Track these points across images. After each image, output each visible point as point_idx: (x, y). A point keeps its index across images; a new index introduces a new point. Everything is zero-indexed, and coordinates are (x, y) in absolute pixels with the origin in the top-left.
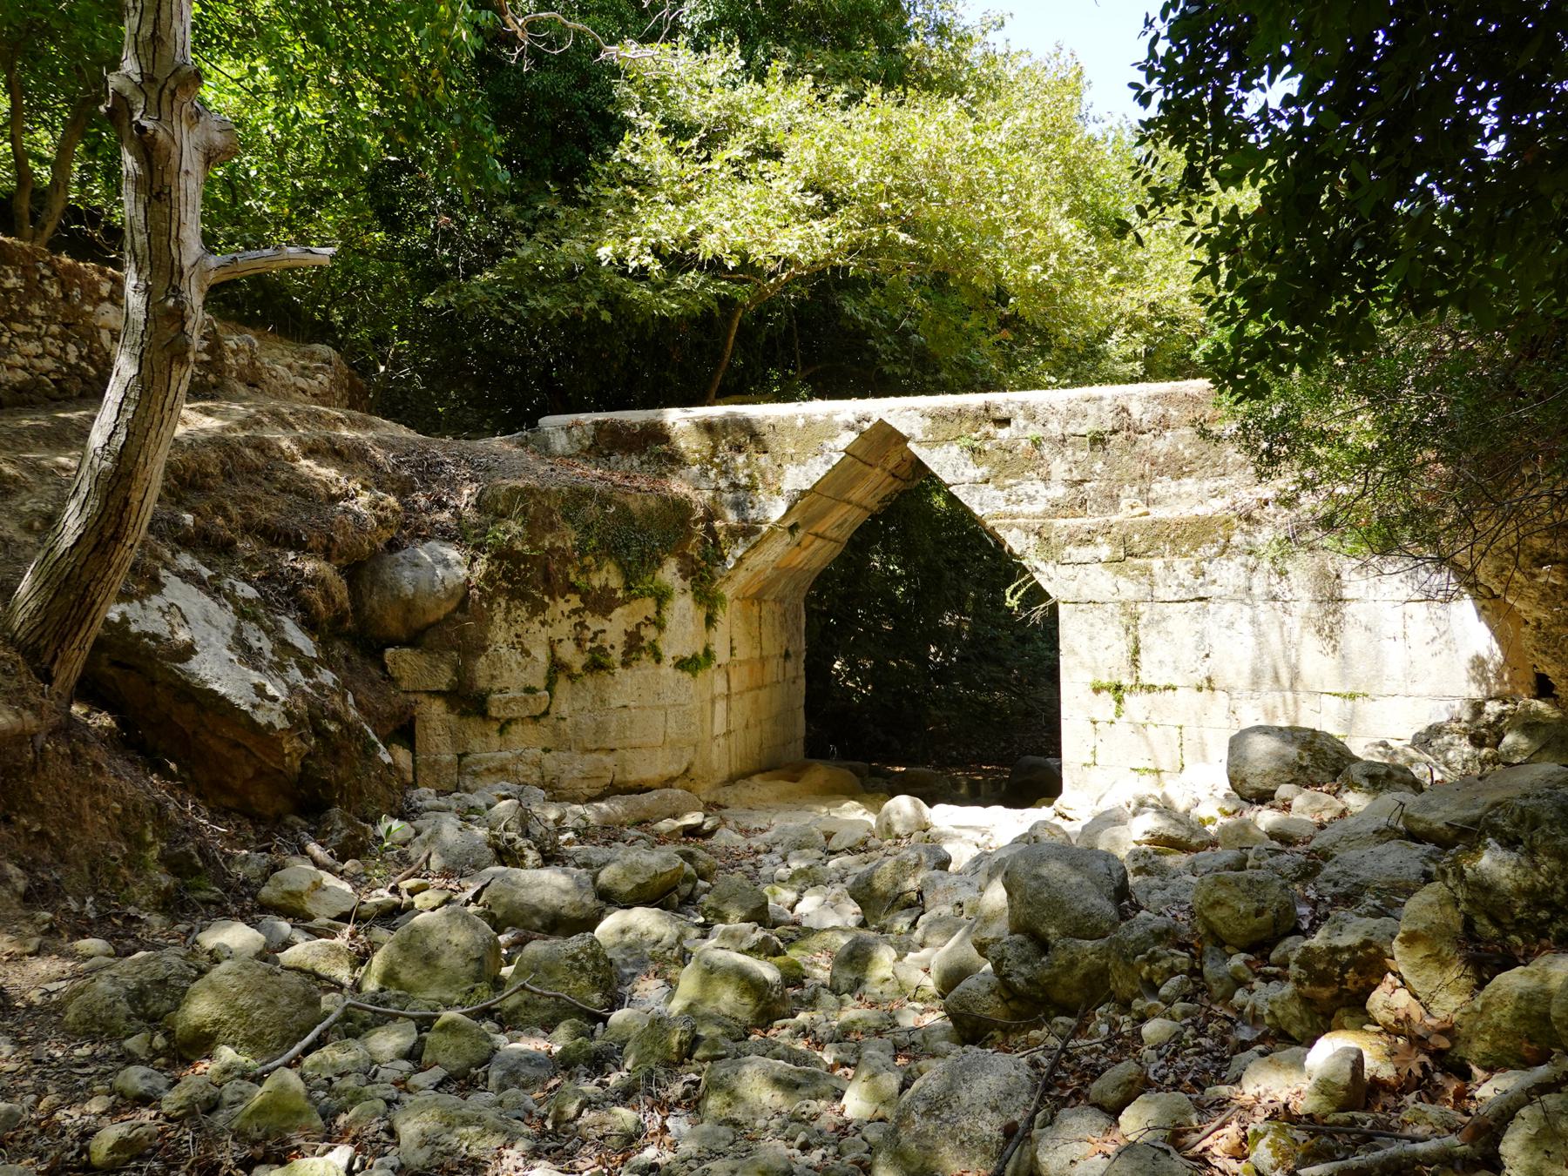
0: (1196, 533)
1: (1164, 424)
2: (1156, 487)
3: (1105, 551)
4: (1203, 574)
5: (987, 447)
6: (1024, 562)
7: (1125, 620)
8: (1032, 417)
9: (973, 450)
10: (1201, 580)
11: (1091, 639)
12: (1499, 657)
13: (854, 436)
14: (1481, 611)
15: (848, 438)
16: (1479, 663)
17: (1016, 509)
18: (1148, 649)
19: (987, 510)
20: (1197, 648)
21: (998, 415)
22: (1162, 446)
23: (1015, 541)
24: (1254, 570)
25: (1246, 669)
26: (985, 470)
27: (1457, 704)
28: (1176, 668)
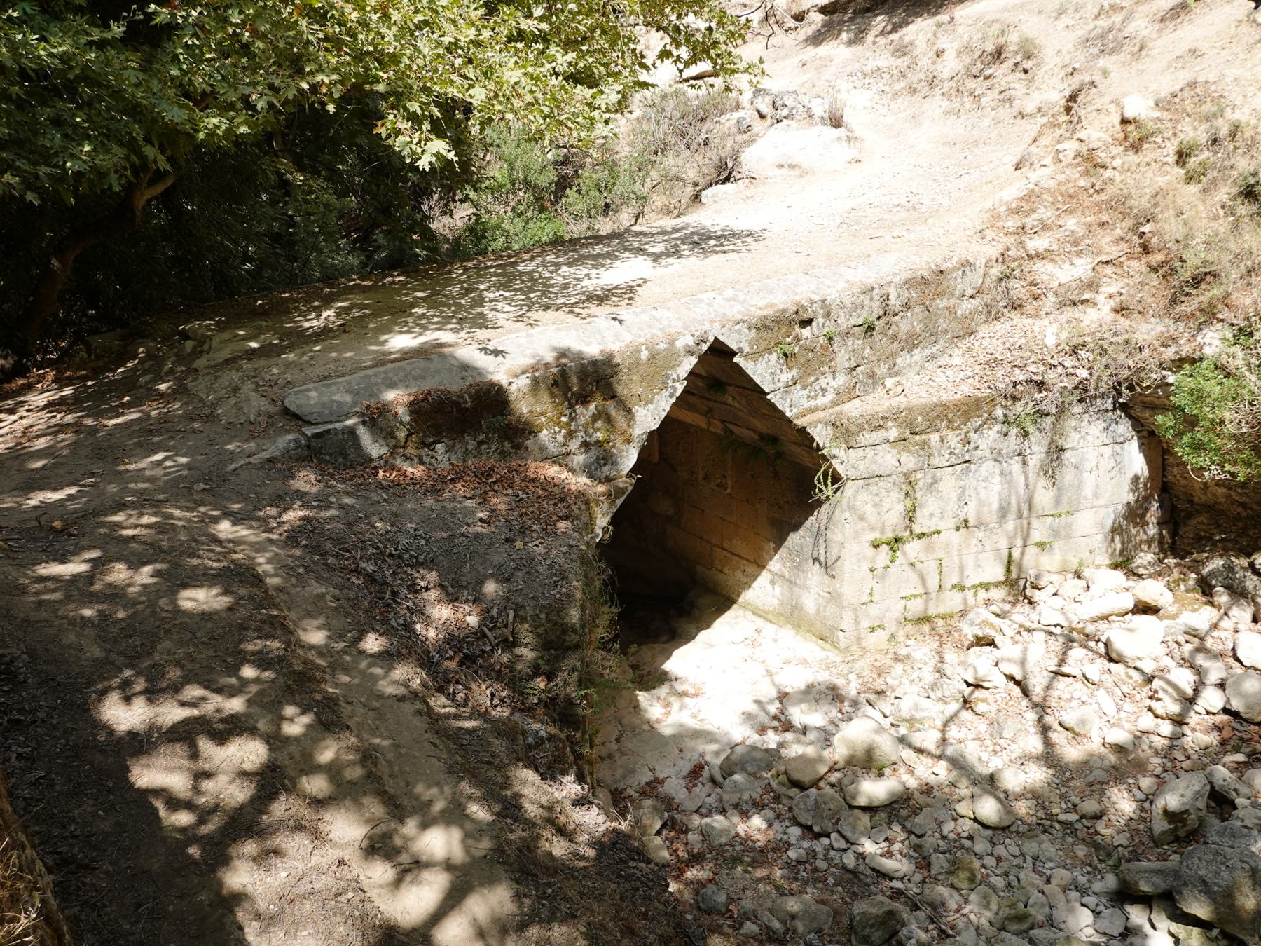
0: (969, 411)
1: (907, 306)
2: (899, 361)
3: (893, 433)
6: (825, 452)
7: (905, 487)
8: (828, 315)
9: (785, 355)
11: (875, 505)
12: (1146, 474)
14: (1141, 445)
15: (689, 363)
16: (1136, 479)
17: (813, 403)
18: (921, 506)
19: (795, 410)
21: (805, 317)
22: (903, 326)
23: (821, 435)
24: (1006, 435)
25: (995, 506)
26: (794, 372)
27: (1120, 507)
28: (942, 517)
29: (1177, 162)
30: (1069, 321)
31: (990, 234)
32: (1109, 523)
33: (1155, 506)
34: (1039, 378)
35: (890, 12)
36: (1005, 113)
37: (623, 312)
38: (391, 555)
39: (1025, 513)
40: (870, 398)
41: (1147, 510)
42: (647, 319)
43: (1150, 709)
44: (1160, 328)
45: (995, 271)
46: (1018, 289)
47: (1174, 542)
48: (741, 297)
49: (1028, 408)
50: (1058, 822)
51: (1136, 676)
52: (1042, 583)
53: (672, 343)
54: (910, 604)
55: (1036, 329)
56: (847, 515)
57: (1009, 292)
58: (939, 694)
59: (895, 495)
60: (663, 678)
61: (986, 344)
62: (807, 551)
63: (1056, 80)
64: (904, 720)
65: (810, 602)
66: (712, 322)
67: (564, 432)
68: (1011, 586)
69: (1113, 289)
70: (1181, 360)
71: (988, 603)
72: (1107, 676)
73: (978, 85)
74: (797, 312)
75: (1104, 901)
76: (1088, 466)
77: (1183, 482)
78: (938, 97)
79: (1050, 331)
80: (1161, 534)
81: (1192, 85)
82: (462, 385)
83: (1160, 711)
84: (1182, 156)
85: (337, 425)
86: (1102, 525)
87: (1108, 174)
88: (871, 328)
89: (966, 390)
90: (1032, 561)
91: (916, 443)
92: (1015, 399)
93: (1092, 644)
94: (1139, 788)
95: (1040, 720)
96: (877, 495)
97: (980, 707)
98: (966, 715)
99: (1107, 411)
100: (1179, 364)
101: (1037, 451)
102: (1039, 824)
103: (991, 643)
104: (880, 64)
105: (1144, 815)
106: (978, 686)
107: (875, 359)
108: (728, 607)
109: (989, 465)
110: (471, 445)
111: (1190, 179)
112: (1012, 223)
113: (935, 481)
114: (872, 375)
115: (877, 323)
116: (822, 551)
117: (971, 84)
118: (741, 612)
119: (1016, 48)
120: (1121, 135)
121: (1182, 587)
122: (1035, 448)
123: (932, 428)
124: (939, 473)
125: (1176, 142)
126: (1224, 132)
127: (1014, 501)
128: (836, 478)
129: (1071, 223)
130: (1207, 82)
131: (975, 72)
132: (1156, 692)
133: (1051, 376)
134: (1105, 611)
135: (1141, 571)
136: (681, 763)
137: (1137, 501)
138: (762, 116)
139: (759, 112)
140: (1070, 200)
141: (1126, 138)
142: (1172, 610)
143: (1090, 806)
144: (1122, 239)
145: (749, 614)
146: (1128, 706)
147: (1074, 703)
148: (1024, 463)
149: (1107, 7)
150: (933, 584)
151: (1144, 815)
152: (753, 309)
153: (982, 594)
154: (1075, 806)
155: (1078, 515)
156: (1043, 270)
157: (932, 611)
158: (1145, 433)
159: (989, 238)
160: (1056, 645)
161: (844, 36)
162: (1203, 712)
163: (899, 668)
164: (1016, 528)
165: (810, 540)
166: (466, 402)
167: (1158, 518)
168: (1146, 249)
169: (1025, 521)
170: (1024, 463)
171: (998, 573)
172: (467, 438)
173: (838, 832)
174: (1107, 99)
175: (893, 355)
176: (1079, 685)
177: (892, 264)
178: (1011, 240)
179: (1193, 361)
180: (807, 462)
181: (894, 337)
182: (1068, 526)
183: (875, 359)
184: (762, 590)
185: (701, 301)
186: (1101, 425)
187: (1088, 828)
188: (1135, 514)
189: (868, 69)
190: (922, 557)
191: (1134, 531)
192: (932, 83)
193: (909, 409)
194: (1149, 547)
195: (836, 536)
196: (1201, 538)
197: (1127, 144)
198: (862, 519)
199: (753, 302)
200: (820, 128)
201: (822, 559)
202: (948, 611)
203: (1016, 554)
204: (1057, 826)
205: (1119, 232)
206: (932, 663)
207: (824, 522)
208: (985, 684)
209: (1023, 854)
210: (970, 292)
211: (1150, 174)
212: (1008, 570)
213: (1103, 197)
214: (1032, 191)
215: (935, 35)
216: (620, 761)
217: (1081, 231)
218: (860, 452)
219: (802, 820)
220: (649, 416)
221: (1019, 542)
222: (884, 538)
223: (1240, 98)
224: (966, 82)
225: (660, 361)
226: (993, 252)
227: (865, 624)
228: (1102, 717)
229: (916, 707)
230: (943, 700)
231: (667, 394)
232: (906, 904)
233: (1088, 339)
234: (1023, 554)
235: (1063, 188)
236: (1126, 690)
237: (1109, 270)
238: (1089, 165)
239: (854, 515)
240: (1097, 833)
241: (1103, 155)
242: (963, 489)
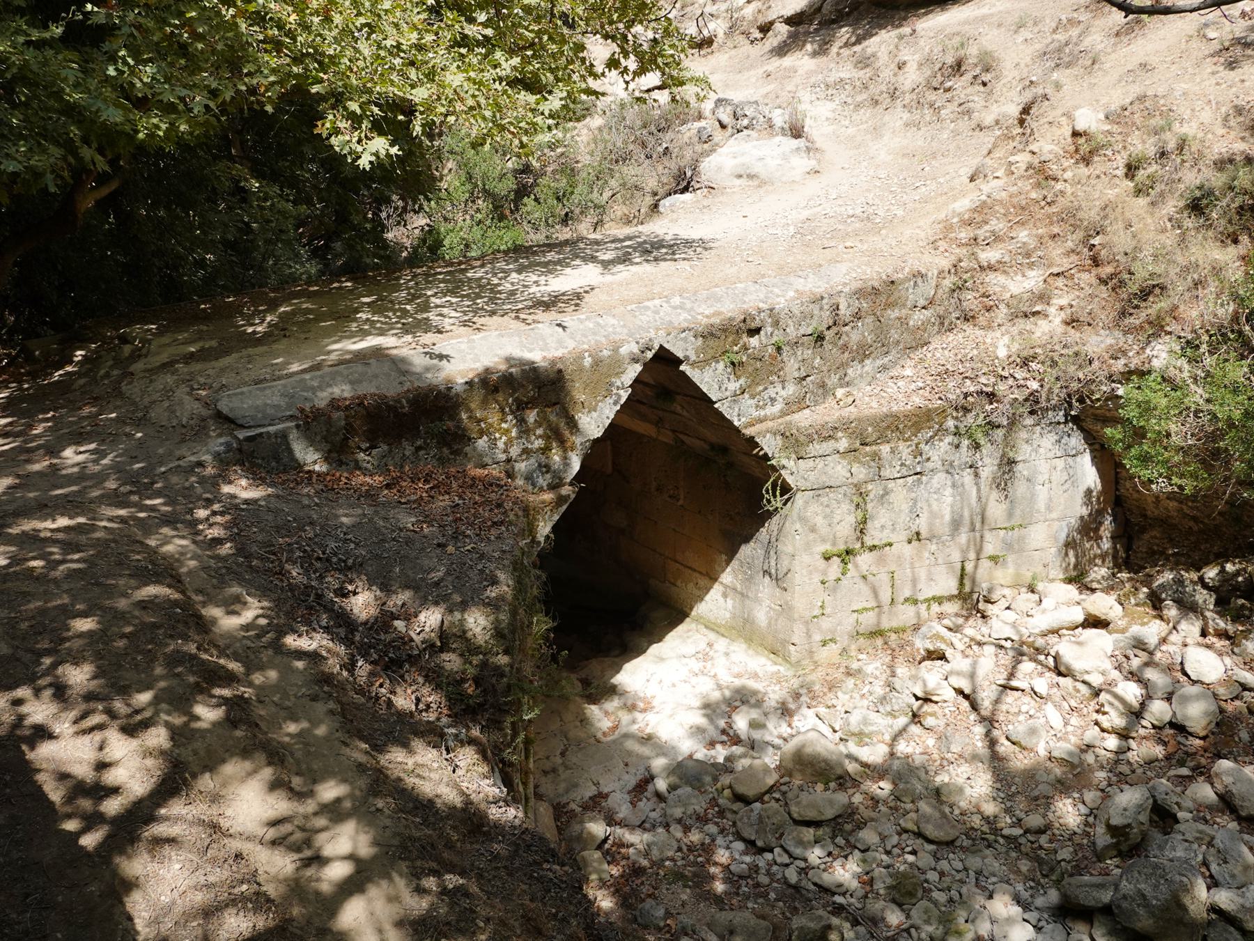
1: (858, 316)
2: (850, 371)
3: (843, 444)
4: (921, 455)
5: (744, 359)
6: (773, 462)
7: (856, 499)
8: (776, 324)
9: (733, 363)
10: (919, 459)
12: (1099, 487)
13: (639, 368)
14: (1093, 459)
15: (634, 371)
16: (1089, 492)
17: (763, 413)
18: (872, 517)
20: (910, 512)
21: (753, 326)
22: (855, 335)
23: (769, 445)
24: (957, 447)
25: (947, 518)
26: (742, 381)
27: (1073, 521)
28: (894, 529)
29: (1126, 175)
30: (1021, 333)
31: (942, 245)
32: (1062, 537)
33: (1108, 521)
34: (989, 389)
35: (855, 24)
36: (964, 124)
37: (567, 319)
38: (319, 559)
39: (978, 526)
40: (820, 409)
41: (1101, 524)
42: (591, 325)
43: (1097, 723)
44: (1110, 341)
45: (948, 283)
46: (970, 300)
47: (1128, 557)
48: (688, 305)
49: (980, 419)
50: (1003, 836)
51: (1084, 689)
52: (994, 597)
53: (616, 350)
54: (862, 618)
55: (988, 341)
56: (798, 526)
57: (962, 302)
58: (888, 709)
59: (846, 506)
60: (613, 691)
61: (938, 355)
62: (758, 563)
63: (1014, 94)
64: (853, 734)
65: (761, 616)
66: (657, 329)
67: (504, 438)
68: (965, 600)
69: (1064, 301)
70: (1130, 373)
71: (941, 616)
72: (1055, 690)
73: (938, 98)
74: (744, 321)
75: (1046, 916)
76: (1041, 479)
77: (1136, 496)
78: (899, 109)
79: (1003, 344)
80: (1115, 548)
81: (1142, 98)
82: (400, 389)
83: (1106, 725)
84: (1131, 169)
85: (271, 429)
86: (1056, 539)
87: (1059, 186)
88: (821, 338)
89: (917, 400)
90: (985, 575)
91: (866, 455)
92: (966, 410)
93: (1042, 657)
94: (1084, 803)
95: (988, 733)
96: (827, 506)
97: (929, 721)
98: (915, 729)
99: (1059, 423)
100: (1127, 376)
101: (989, 465)
102: (983, 839)
103: (942, 657)
104: (842, 75)
105: (1088, 829)
106: (927, 700)
107: (825, 369)
108: (680, 621)
109: (940, 477)
110: (409, 451)
111: (1138, 192)
112: (964, 235)
113: (886, 493)
114: (823, 385)
115: (826, 333)
116: (773, 563)
117: (931, 96)
118: (693, 625)
119: (975, 61)
120: (1072, 148)
121: (1133, 601)
122: (987, 461)
123: (882, 439)
124: (891, 485)
125: (1125, 155)
126: (1171, 146)
127: (966, 514)
128: (786, 489)
129: (1023, 235)
130: (1156, 96)
131: (935, 84)
132: (1102, 705)
133: (1002, 388)
134: (1055, 625)
135: (1095, 585)
136: (626, 777)
137: (1090, 515)
138: (723, 126)
139: (720, 122)
140: (1022, 212)
141: (1077, 151)
142: (1122, 623)
143: (1035, 821)
144: (1073, 251)
145: (702, 628)
146: (1075, 720)
147: (1021, 718)
148: (977, 475)
149: (1065, 21)
150: (885, 596)
151: (1088, 829)
152: (700, 317)
153: (935, 608)
154: (1020, 820)
155: (1031, 528)
156: (995, 281)
157: (885, 625)
158: (1097, 446)
159: (941, 249)
160: (1006, 659)
161: (809, 47)
162: (1149, 726)
163: (850, 682)
164: (969, 541)
165: (761, 552)
166: (403, 407)
167: (1112, 532)
168: (1096, 262)
169: (978, 535)
170: (977, 475)
171: (951, 586)
172: (405, 443)
173: (782, 847)
174: (1059, 112)
175: (844, 365)
176: (1027, 699)
177: (844, 274)
178: (963, 251)
179: (1142, 374)
180: (757, 472)
181: (845, 347)
182: (1021, 539)
183: (825, 369)
184: (715, 603)
185: (648, 308)
186: (1053, 437)
187: (1032, 843)
188: (1088, 528)
189: (831, 80)
190: (874, 569)
191: (1088, 545)
192: (893, 94)
193: (859, 420)
194: (1103, 562)
195: (786, 547)
196: (1154, 553)
197: (1078, 156)
198: (813, 530)
199: (701, 310)
200: (779, 138)
201: (773, 571)
202: (901, 624)
203: (969, 567)
204: (1001, 840)
205: (1070, 244)
206: (884, 677)
207: (775, 533)
208: (934, 698)
209: (966, 869)
210: (922, 302)
211: (1099, 187)
212: (962, 584)
213: (1054, 209)
214: (984, 202)
215: (897, 47)
216: (564, 775)
217: (1032, 243)
218: (810, 463)
219: (745, 835)
220: (594, 421)
221: (972, 556)
222: (835, 550)
223: (1189, 112)
224: (927, 94)
225: (604, 368)
226: (945, 263)
227: (817, 637)
228: (1049, 727)
229: (865, 721)
230: (891, 714)
231: (611, 401)
232: (847, 919)
233: (1039, 351)
234: (976, 567)
235: (1015, 200)
236: (1073, 704)
237: (1060, 282)
238: (1041, 177)
239: (805, 527)
240: (1041, 847)
241: (1054, 167)
242: (915, 501)
